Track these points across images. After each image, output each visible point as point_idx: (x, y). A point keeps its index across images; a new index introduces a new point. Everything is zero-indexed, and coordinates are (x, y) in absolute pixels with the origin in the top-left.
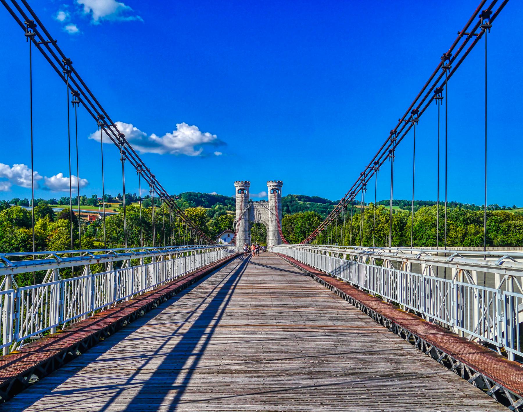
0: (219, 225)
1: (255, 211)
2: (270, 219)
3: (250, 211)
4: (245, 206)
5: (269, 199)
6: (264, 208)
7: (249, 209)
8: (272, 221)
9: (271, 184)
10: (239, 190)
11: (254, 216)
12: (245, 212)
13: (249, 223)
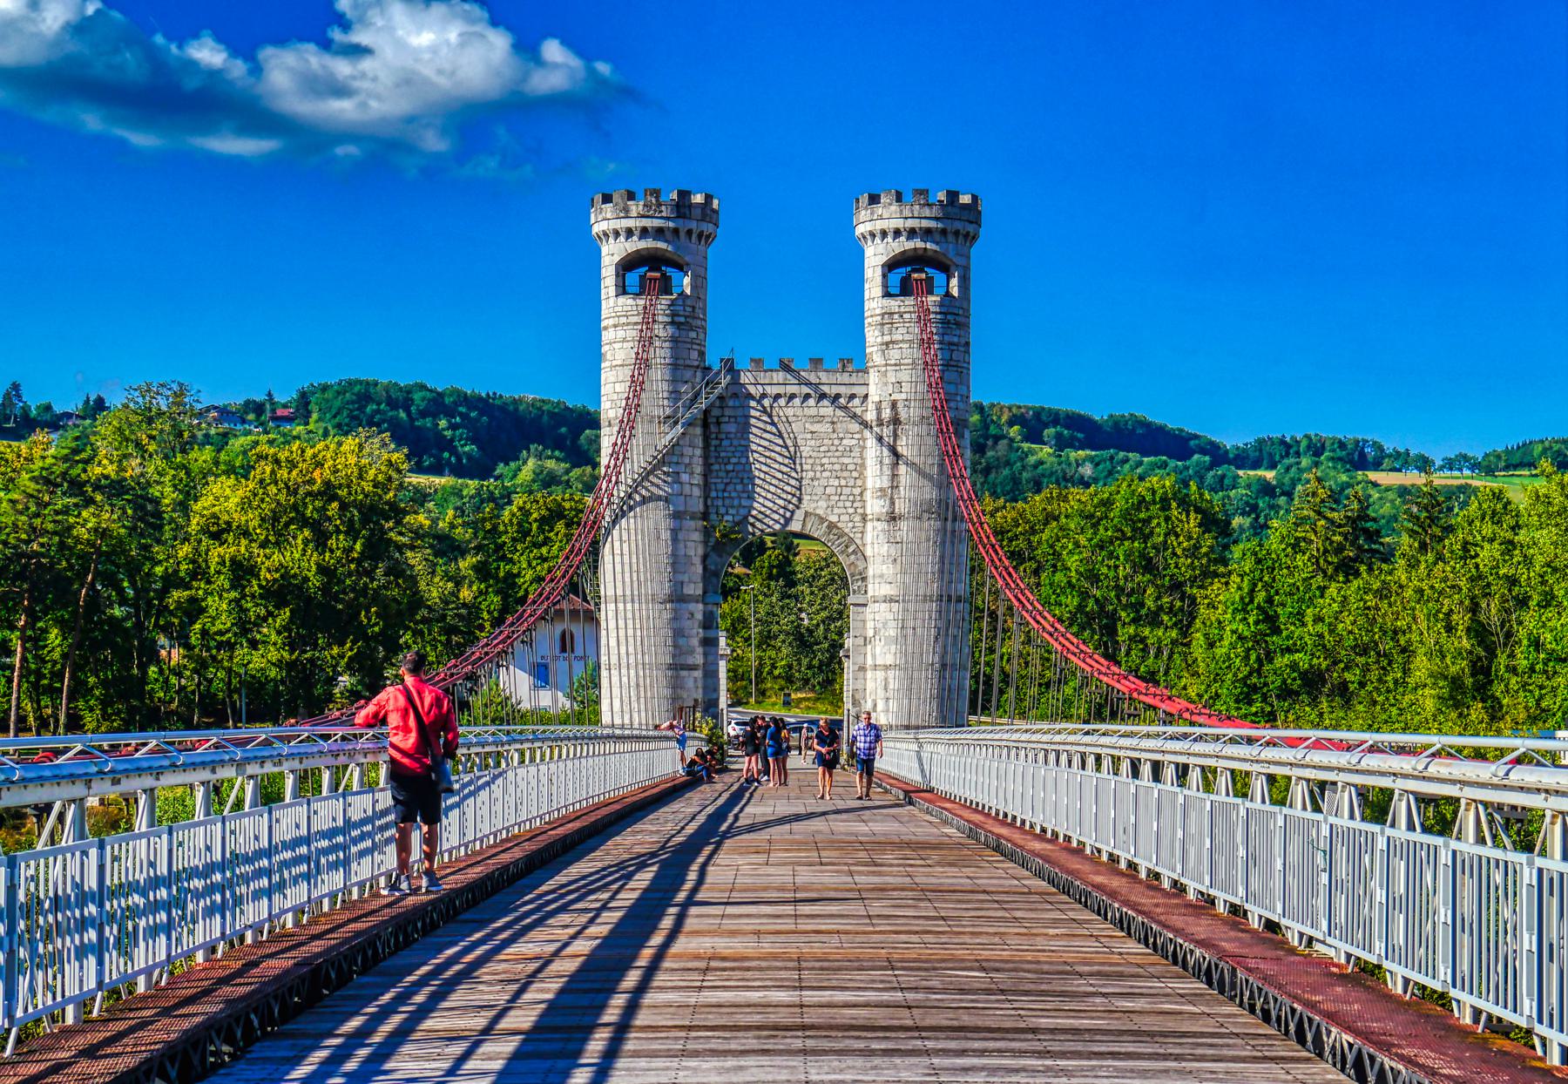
0: (504, 569)
1: (757, 441)
2: (875, 506)
3: (717, 427)
4: (675, 395)
5: (873, 337)
6: (827, 409)
7: (707, 421)
8: (893, 518)
9: (889, 215)
10: (627, 265)
11: (745, 477)
12: (674, 449)
13: (707, 532)
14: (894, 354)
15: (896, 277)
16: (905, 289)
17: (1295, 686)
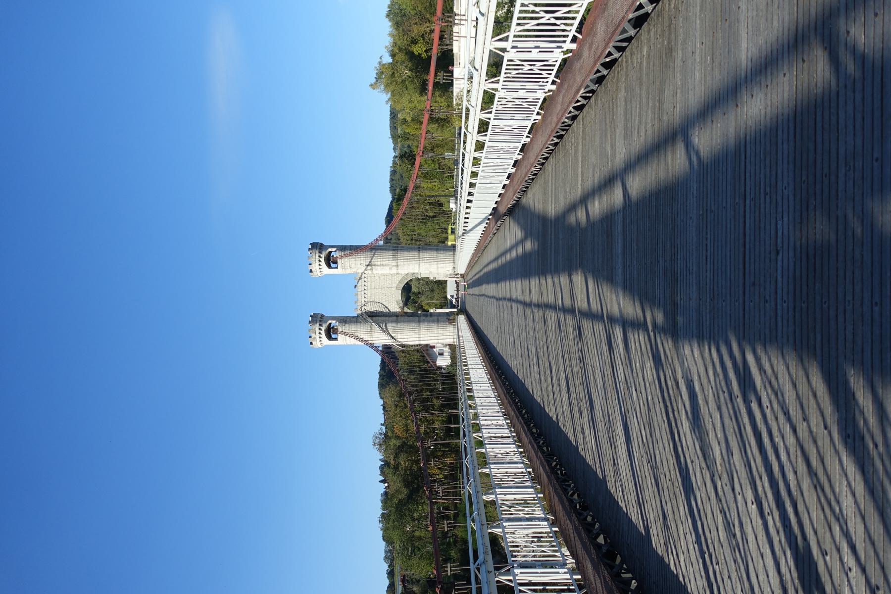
2: (394, 271)
5: (348, 271)
9: (315, 267)
14: (353, 266)
15: (333, 265)
16: (336, 263)
17: (446, 173)
